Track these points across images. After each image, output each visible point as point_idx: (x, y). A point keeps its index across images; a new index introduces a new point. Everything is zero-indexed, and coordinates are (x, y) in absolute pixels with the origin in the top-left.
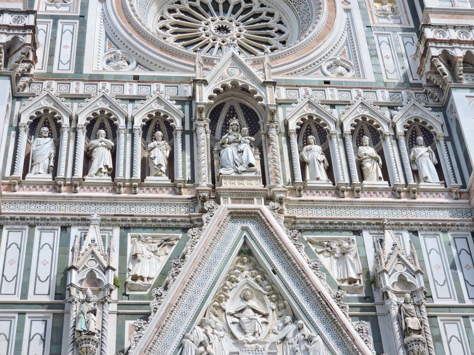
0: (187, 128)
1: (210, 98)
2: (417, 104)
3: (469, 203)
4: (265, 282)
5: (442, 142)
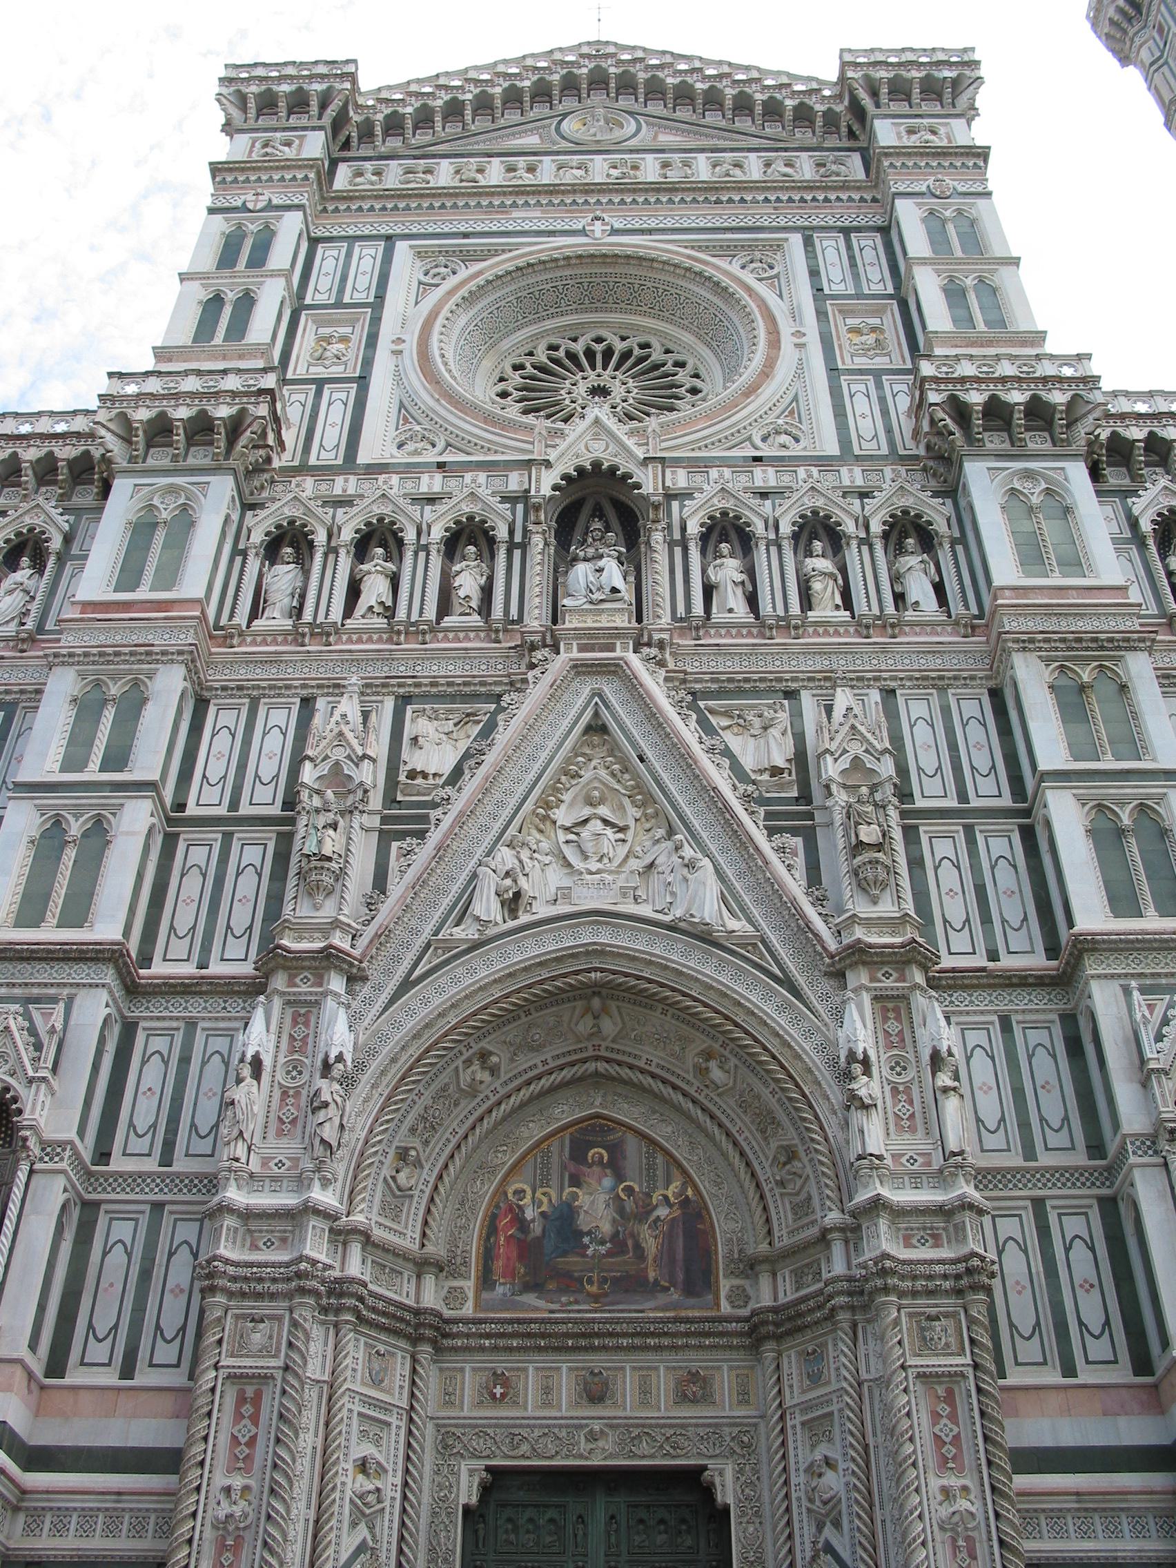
0: (518, 538)
1: (555, 488)
2: (907, 486)
3: (988, 642)
4: (627, 776)
5: (947, 546)
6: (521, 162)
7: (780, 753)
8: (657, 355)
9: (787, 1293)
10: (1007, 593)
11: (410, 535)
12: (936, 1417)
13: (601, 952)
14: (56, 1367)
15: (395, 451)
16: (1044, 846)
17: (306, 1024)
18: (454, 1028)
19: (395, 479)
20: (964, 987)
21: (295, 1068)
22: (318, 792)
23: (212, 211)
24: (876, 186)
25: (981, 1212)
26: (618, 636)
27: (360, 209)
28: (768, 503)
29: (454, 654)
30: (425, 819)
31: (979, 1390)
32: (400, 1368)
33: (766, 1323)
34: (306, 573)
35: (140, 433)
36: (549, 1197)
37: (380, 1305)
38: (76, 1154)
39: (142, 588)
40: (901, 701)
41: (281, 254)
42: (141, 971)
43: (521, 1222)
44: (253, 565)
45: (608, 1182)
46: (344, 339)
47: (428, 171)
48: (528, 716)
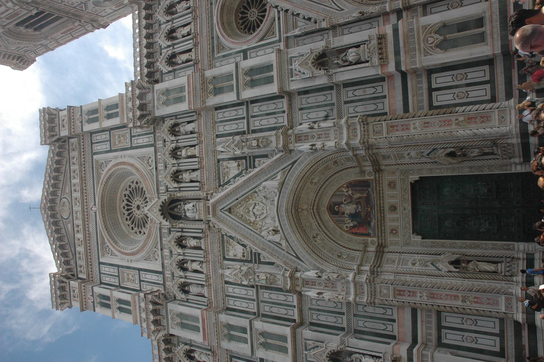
1: (167, 221)
4: (242, 203)
5: (178, 120)
6: (76, 229)
7: (234, 164)
8: (128, 193)
9: (369, 163)
10: (190, 106)
11: (181, 257)
12: (397, 130)
13: (287, 210)
14: (394, 337)
15: (158, 261)
16: (256, 98)
17: (308, 282)
18: (307, 245)
19: (166, 261)
20: (292, 119)
21: (320, 284)
22: (250, 280)
23: (94, 310)
24: (79, 135)
25: (348, 118)
26: (205, 205)
27: (91, 271)
28: (168, 166)
29: (211, 246)
30: (255, 253)
31: (391, 120)
32: (390, 256)
33: (376, 169)
34: (191, 283)
35: (157, 328)
36: (347, 220)
37: (376, 261)
38: (343, 336)
39: (199, 325)
40: (219, 133)
41: (106, 292)
42: (297, 322)
43: (354, 227)
44: (190, 297)
45: (343, 206)
46: (128, 275)
47: (80, 253)
48: (228, 228)
